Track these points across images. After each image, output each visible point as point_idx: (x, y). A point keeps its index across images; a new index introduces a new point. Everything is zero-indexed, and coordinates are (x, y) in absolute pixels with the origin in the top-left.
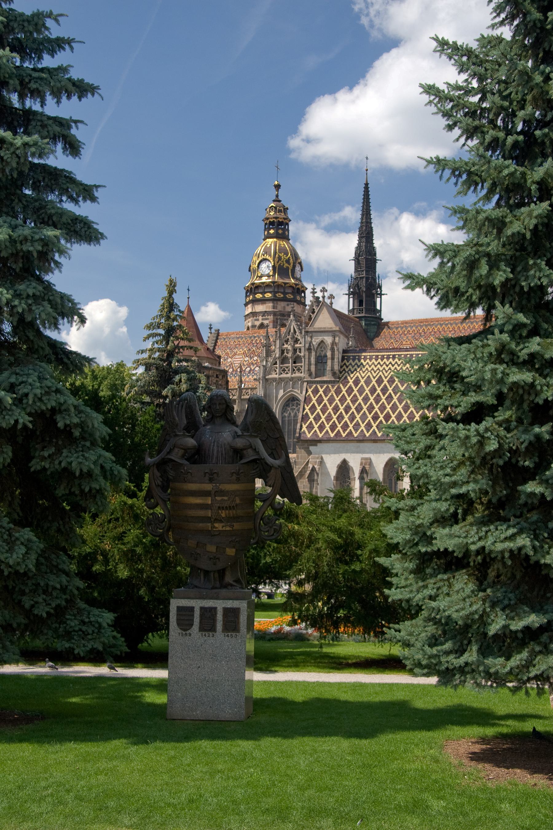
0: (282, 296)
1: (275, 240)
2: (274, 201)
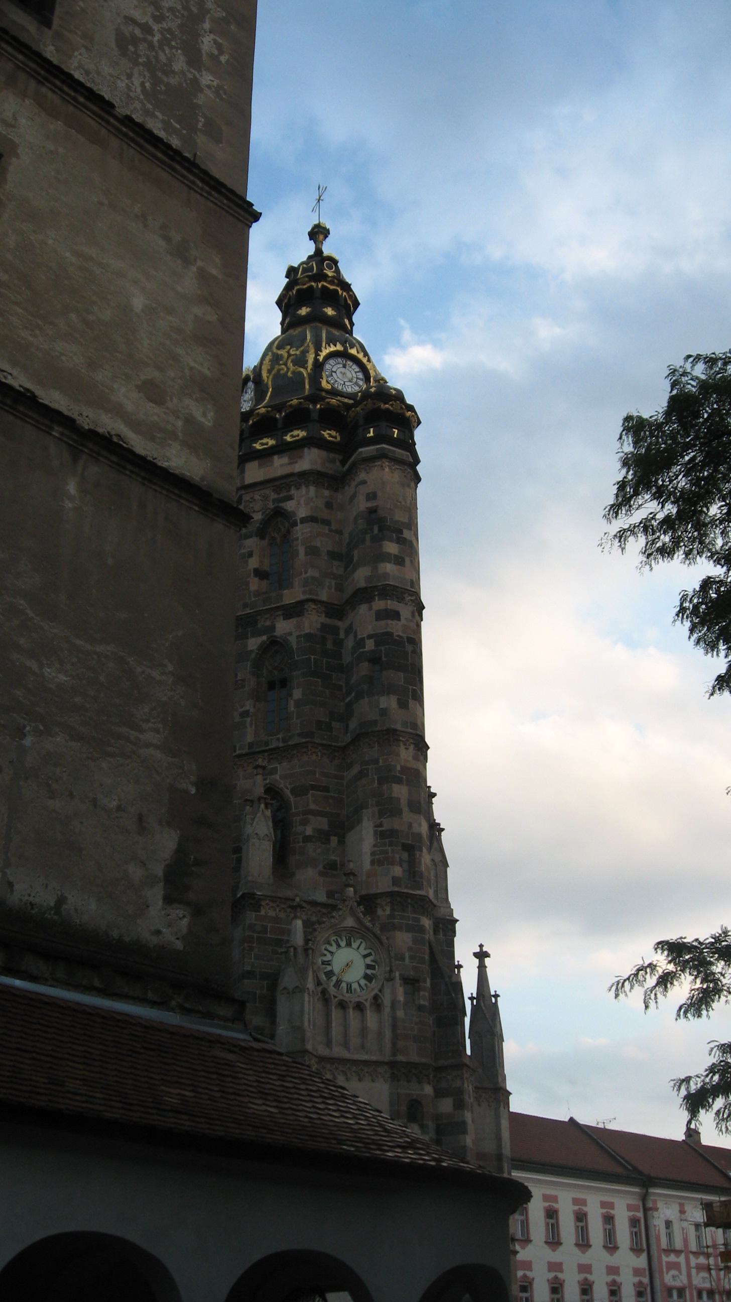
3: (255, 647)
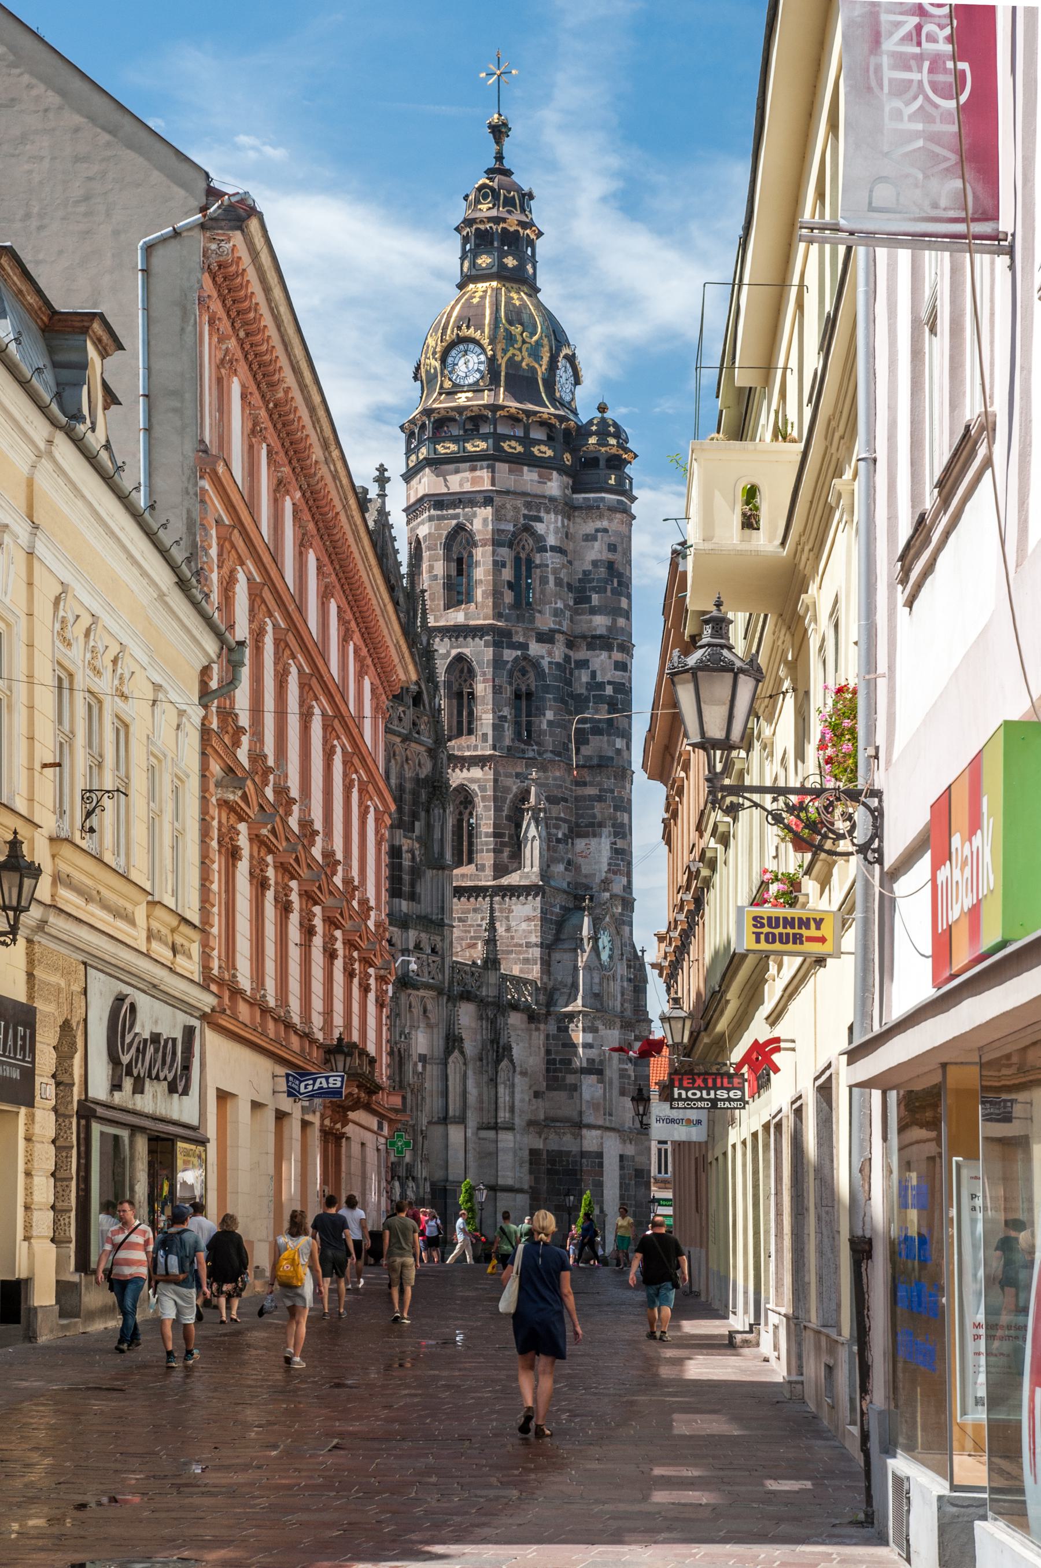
0: (520, 449)
1: (494, 284)
2: (490, 172)
3: (510, 659)
